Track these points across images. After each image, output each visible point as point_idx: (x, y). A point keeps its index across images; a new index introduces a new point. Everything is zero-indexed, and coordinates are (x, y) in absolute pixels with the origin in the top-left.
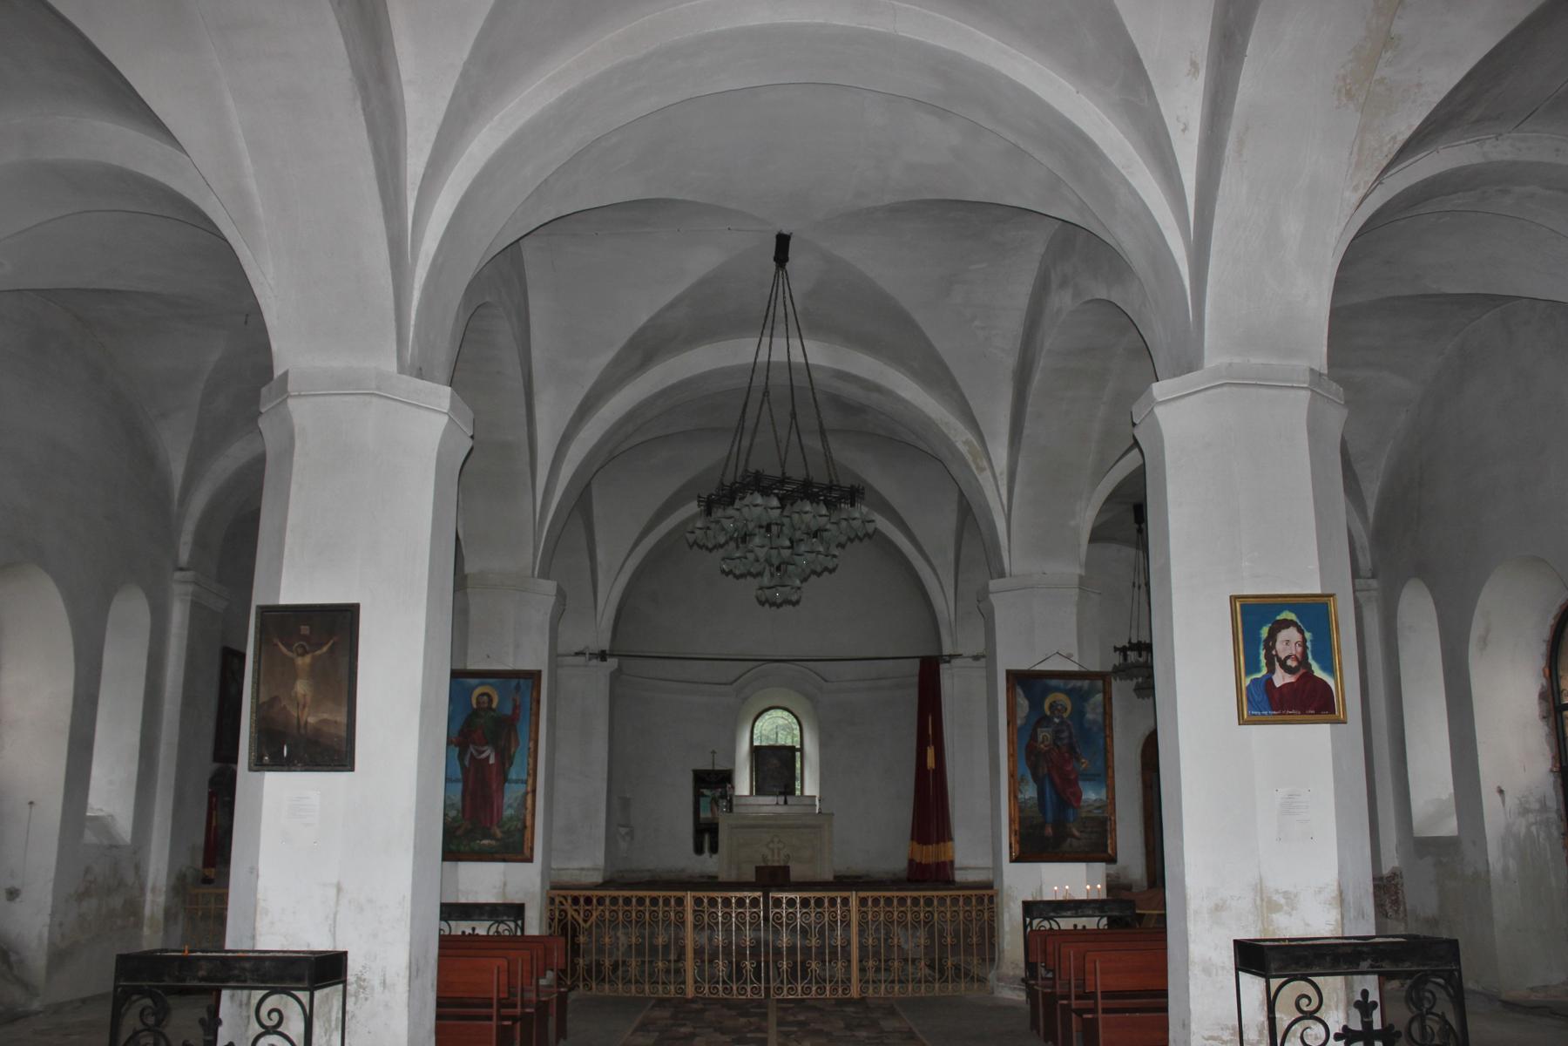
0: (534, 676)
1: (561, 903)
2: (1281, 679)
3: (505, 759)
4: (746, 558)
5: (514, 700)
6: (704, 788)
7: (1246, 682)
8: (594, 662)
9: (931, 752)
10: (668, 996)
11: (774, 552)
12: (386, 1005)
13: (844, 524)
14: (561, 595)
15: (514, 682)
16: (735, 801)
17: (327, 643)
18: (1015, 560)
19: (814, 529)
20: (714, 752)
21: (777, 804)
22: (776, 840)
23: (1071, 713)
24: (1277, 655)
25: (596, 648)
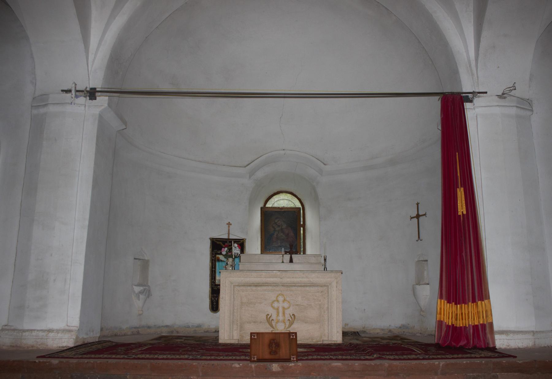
8: (82, 100)
9: (461, 193)
20: (229, 224)
22: (281, 299)
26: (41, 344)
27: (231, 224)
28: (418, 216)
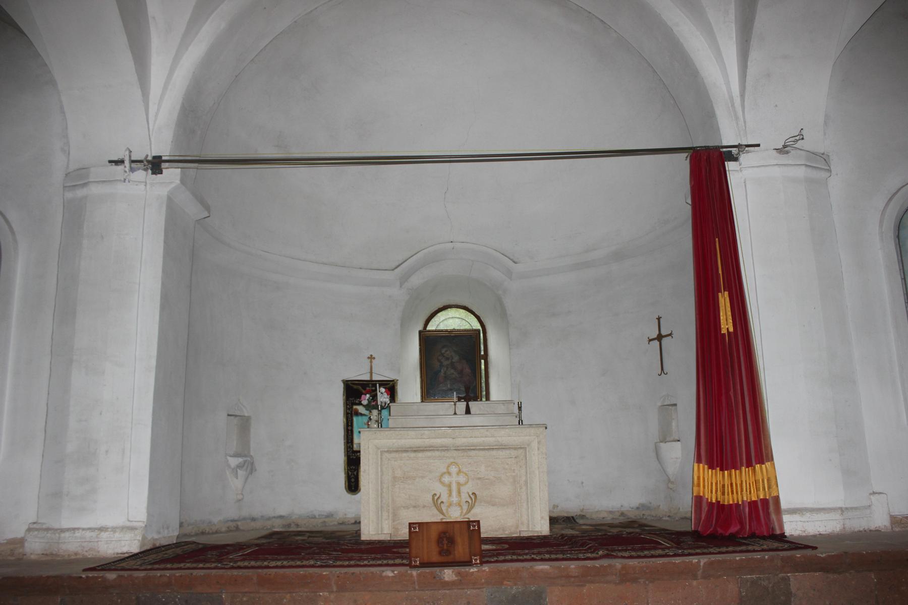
8: (141, 175)
9: (724, 300)
20: (371, 358)
22: (454, 469)
26: (89, 550)
27: (374, 358)
28: (660, 337)
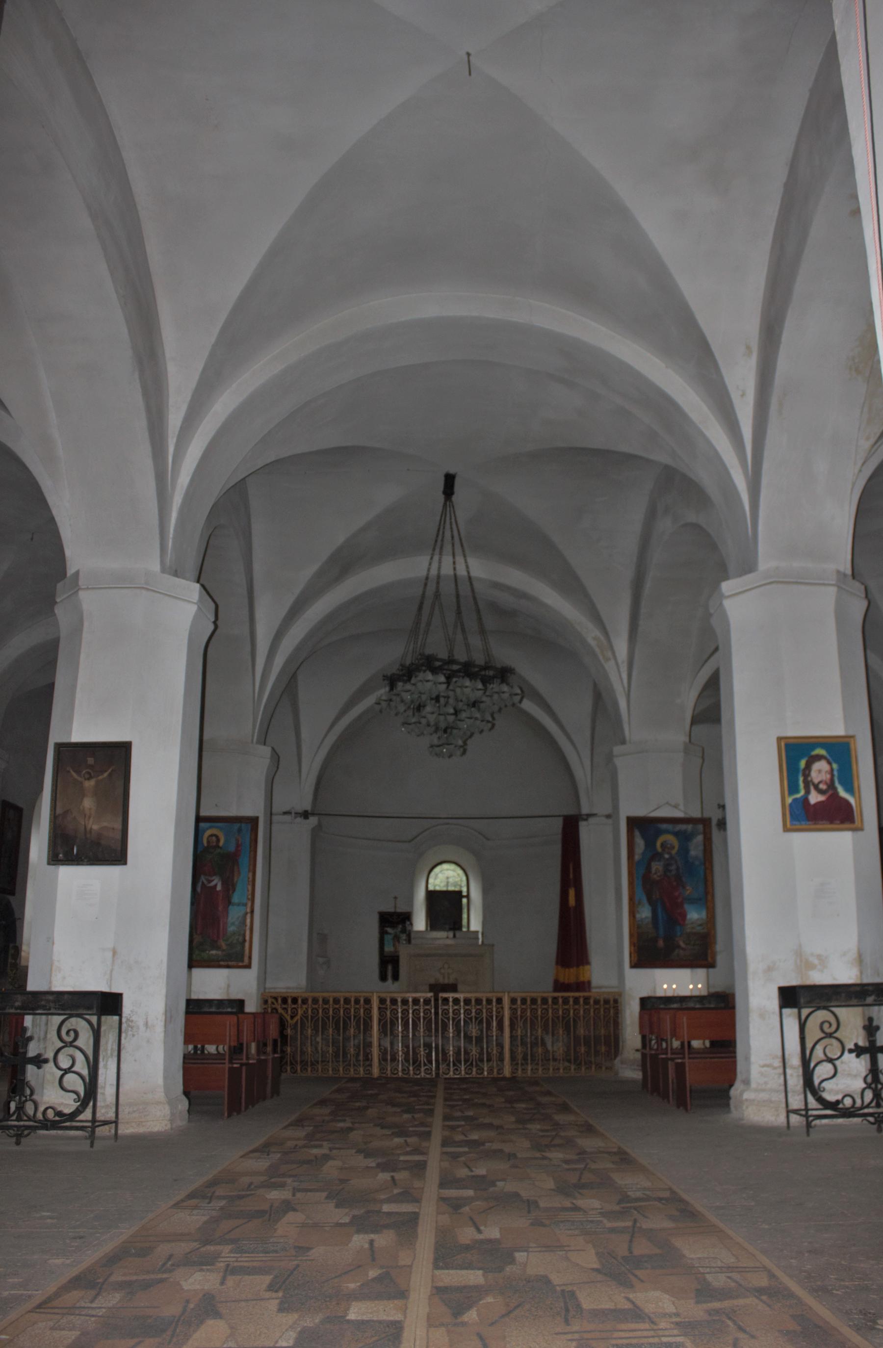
0: (253, 822)
1: (273, 1003)
2: (815, 798)
3: (229, 886)
4: (420, 723)
5: (237, 840)
6: (388, 927)
7: (789, 800)
9: (572, 892)
10: (357, 1076)
11: (442, 718)
12: (148, 1041)
13: (496, 697)
14: (276, 757)
15: (236, 826)
16: (413, 935)
17: (106, 771)
18: (633, 730)
19: (473, 700)
20: (396, 898)
21: (447, 938)
22: (446, 966)
23: (678, 851)
24: (812, 781)
25: (300, 808)
